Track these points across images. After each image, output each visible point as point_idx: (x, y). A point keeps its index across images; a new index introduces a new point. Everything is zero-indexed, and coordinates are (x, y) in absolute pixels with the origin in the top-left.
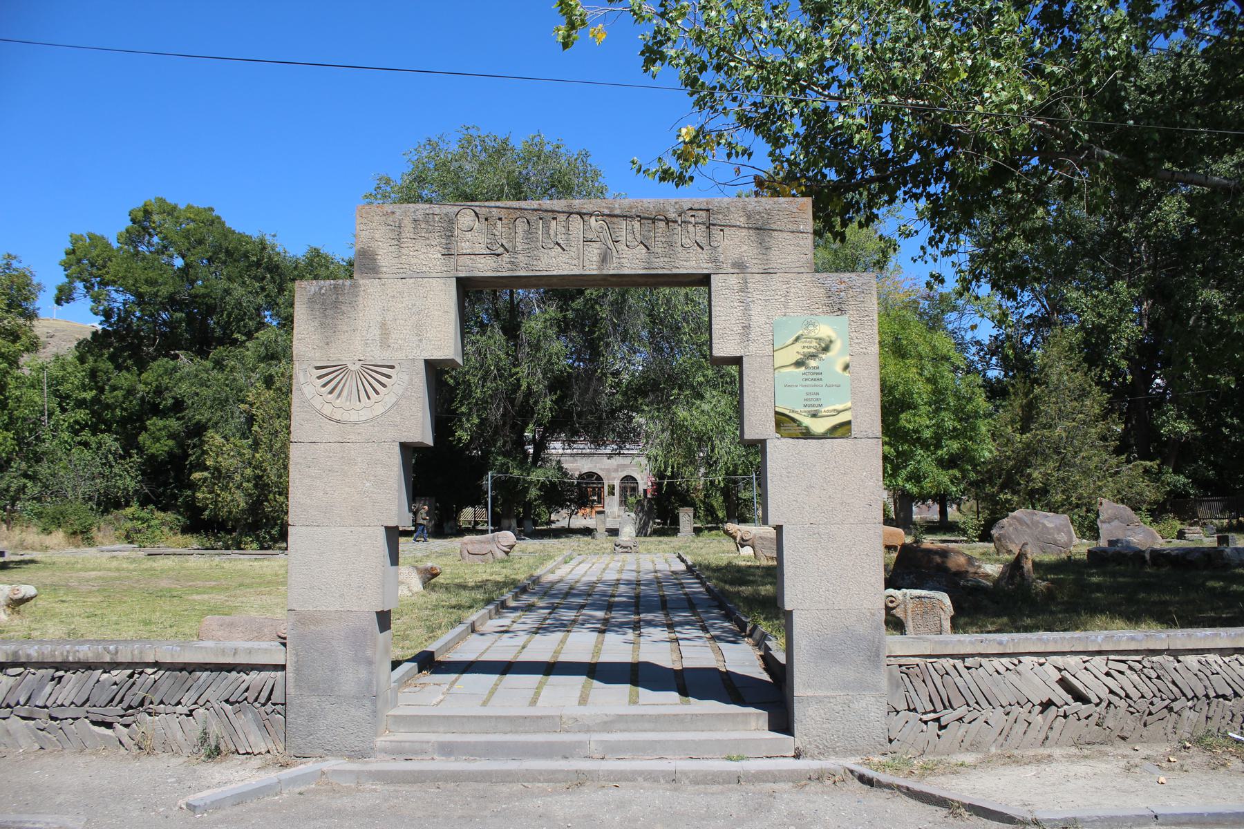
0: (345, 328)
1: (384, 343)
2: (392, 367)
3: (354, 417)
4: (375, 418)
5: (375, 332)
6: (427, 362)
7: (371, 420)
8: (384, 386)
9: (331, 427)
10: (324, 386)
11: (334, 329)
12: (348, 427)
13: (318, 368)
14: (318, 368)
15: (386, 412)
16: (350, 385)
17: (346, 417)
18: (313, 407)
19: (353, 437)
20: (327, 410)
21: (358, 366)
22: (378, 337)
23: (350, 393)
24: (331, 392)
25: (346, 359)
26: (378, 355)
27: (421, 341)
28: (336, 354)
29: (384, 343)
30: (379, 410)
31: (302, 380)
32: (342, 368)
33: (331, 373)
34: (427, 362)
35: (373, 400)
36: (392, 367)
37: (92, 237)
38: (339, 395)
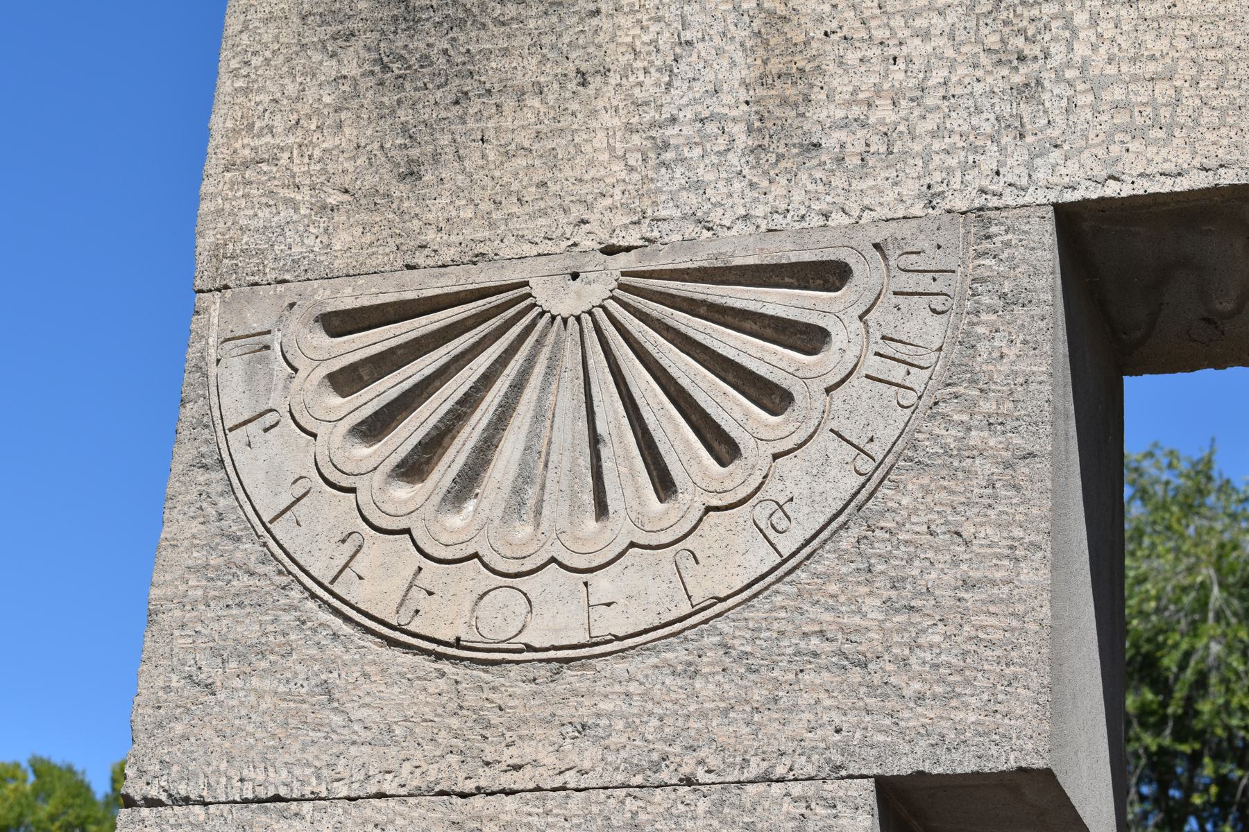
0: (528, 70)
1: (778, 131)
2: (831, 275)
3: (556, 615)
4: (708, 611)
5: (728, 70)
6: (1069, 218)
7: (671, 628)
8: (770, 396)
9: (393, 689)
10: (373, 428)
11: (465, 87)
12: (512, 684)
13: (340, 323)
14: (340, 323)
15: (785, 567)
16: (551, 411)
17: (501, 619)
18: (291, 567)
19: (542, 756)
20: (379, 581)
21: (597, 288)
22: (732, 103)
23: (524, 477)
24: (413, 468)
25: (519, 254)
26: (741, 212)
27: (1029, 91)
28: (465, 227)
29: (778, 131)
30: (733, 555)
31: (235, 400)
32: (503, 310)
33: (428, 364)
34: (1069, 218)
35: (690, 499)
36: (831, 275)
37: (41, 768)
38: (467, 484)
